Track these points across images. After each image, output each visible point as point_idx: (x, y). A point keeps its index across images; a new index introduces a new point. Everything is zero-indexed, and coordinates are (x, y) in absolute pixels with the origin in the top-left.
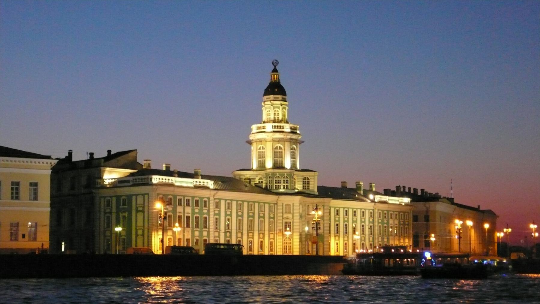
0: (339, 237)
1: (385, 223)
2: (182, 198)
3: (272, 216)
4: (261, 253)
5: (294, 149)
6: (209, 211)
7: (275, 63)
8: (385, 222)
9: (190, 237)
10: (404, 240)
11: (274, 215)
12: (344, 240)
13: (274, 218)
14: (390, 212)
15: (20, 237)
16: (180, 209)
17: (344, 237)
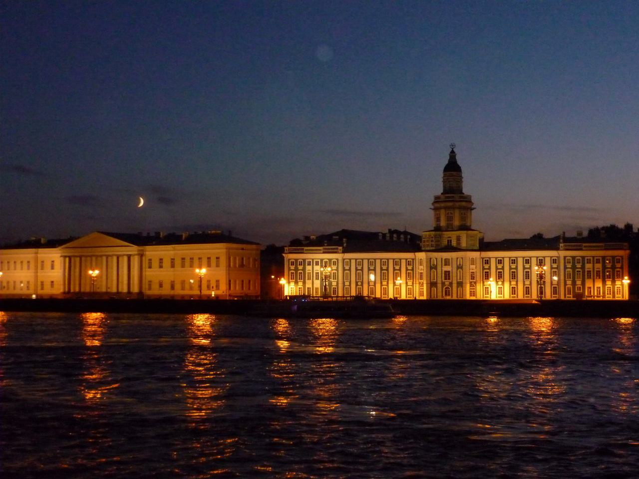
0: (503, 282)
1: (578, 268)
2: (311, 260)
3: (410, 267)
4: (384, 297)
5: (451, 214)
6: (338, 267)
7: (453, 146)
8: (579, 266)
9: (319, 286)
10: (614, 282)
11: (413, 268)
12: (510, 284)
13: (413, 270)
14: (586, 258)
15: (211, 288)
16: (308, 268)
17: (510, 282)
